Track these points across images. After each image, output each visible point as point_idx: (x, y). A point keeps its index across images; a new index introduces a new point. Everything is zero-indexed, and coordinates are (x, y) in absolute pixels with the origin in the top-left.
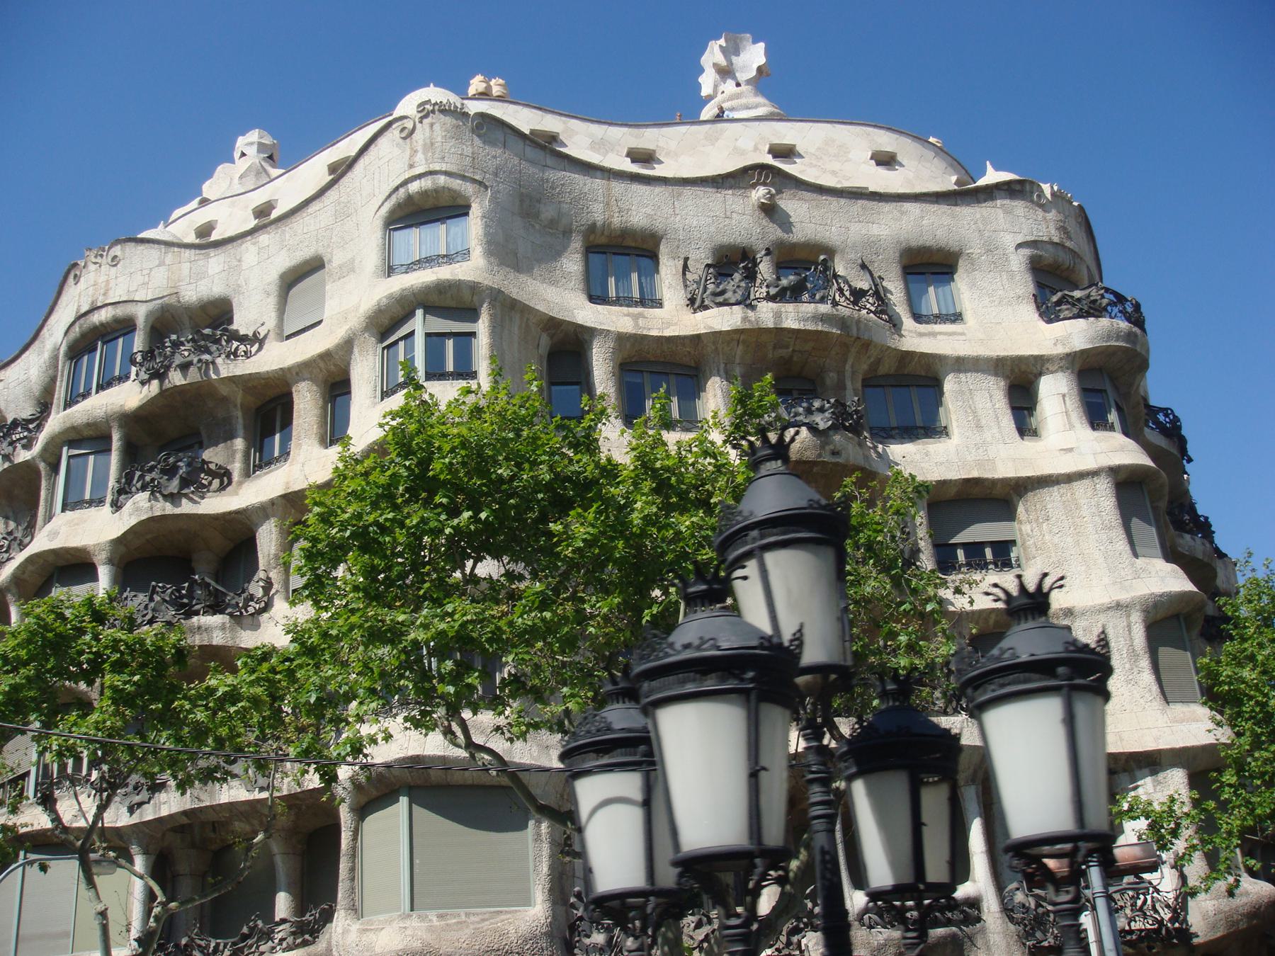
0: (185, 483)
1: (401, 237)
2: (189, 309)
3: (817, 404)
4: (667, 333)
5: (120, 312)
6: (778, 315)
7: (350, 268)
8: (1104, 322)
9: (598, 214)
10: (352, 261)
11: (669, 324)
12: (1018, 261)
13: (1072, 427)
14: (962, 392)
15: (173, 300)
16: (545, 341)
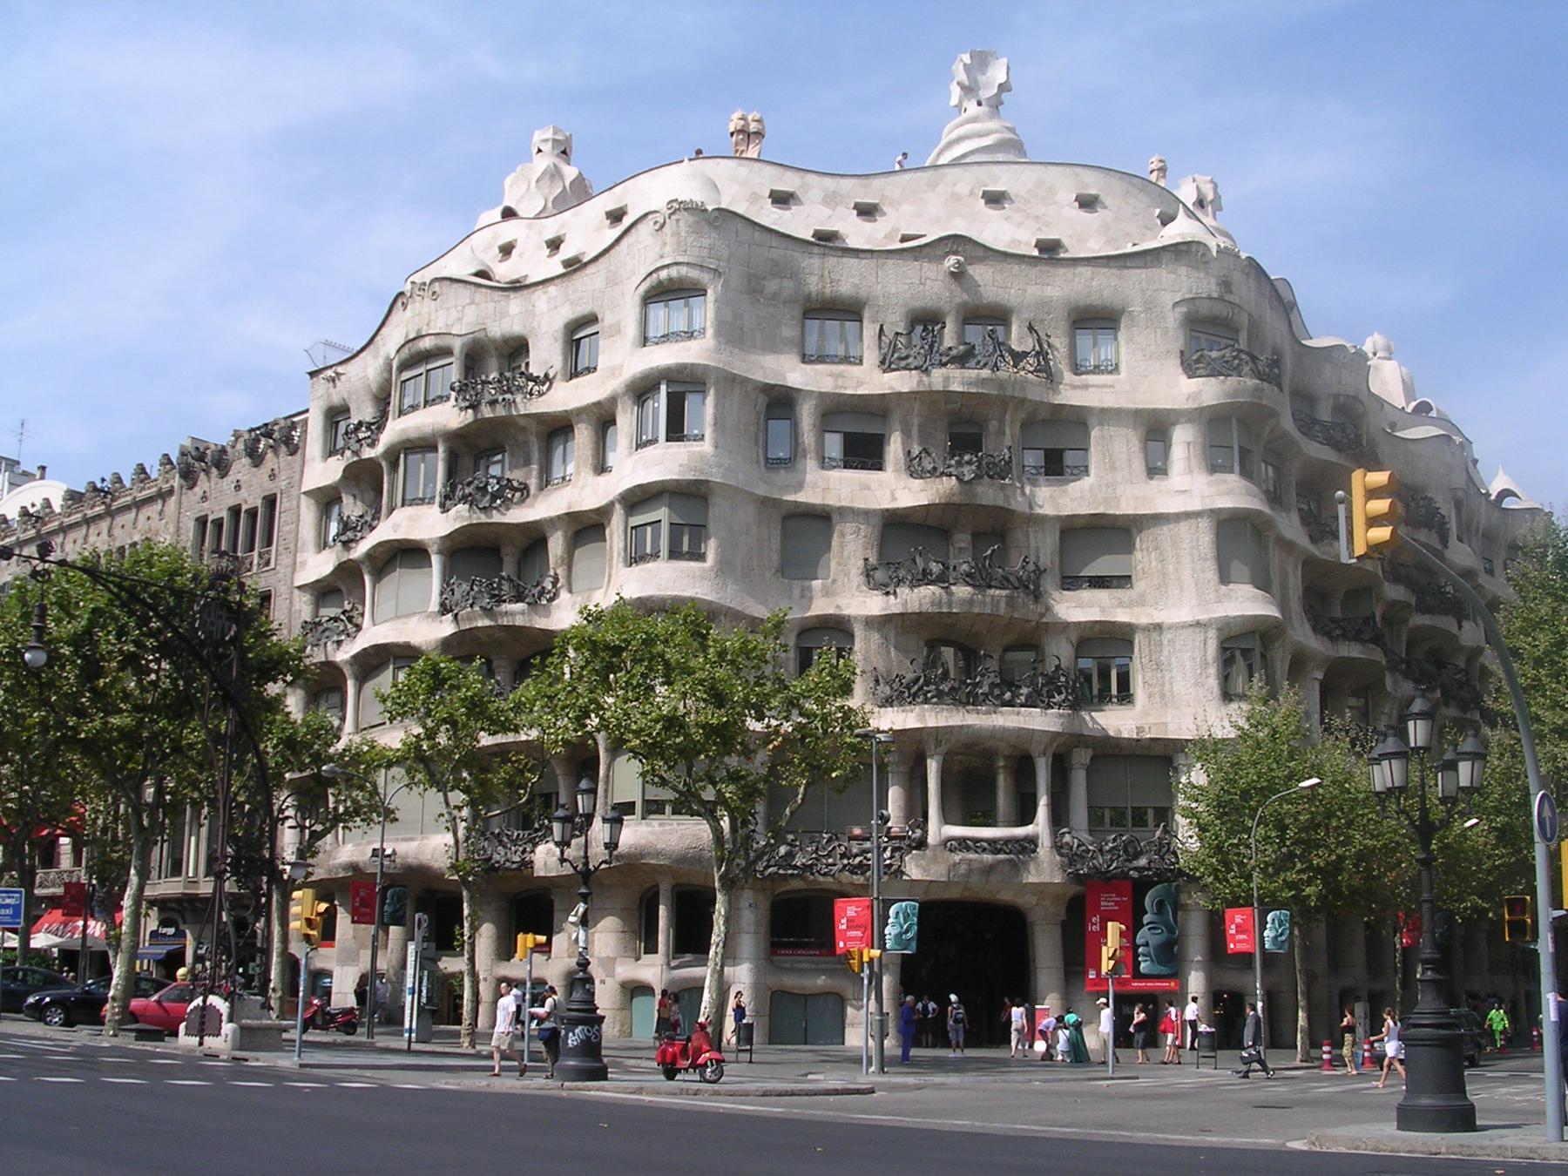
0: (494, 497)
1: (658, 312)
2: (493, 341)
3: (967, 458)
4: (860, 391)
5: (440, 342)
6: (947, 379)
7: (617, 330)
8: (1233, 381)
9: (813, 285)
10: (619, 323)
11: (860, 384)
12: (1173, 318)
13: (1190, 471)
14: (1103, 438)
15: (482, 335)
16: (762, 400)
